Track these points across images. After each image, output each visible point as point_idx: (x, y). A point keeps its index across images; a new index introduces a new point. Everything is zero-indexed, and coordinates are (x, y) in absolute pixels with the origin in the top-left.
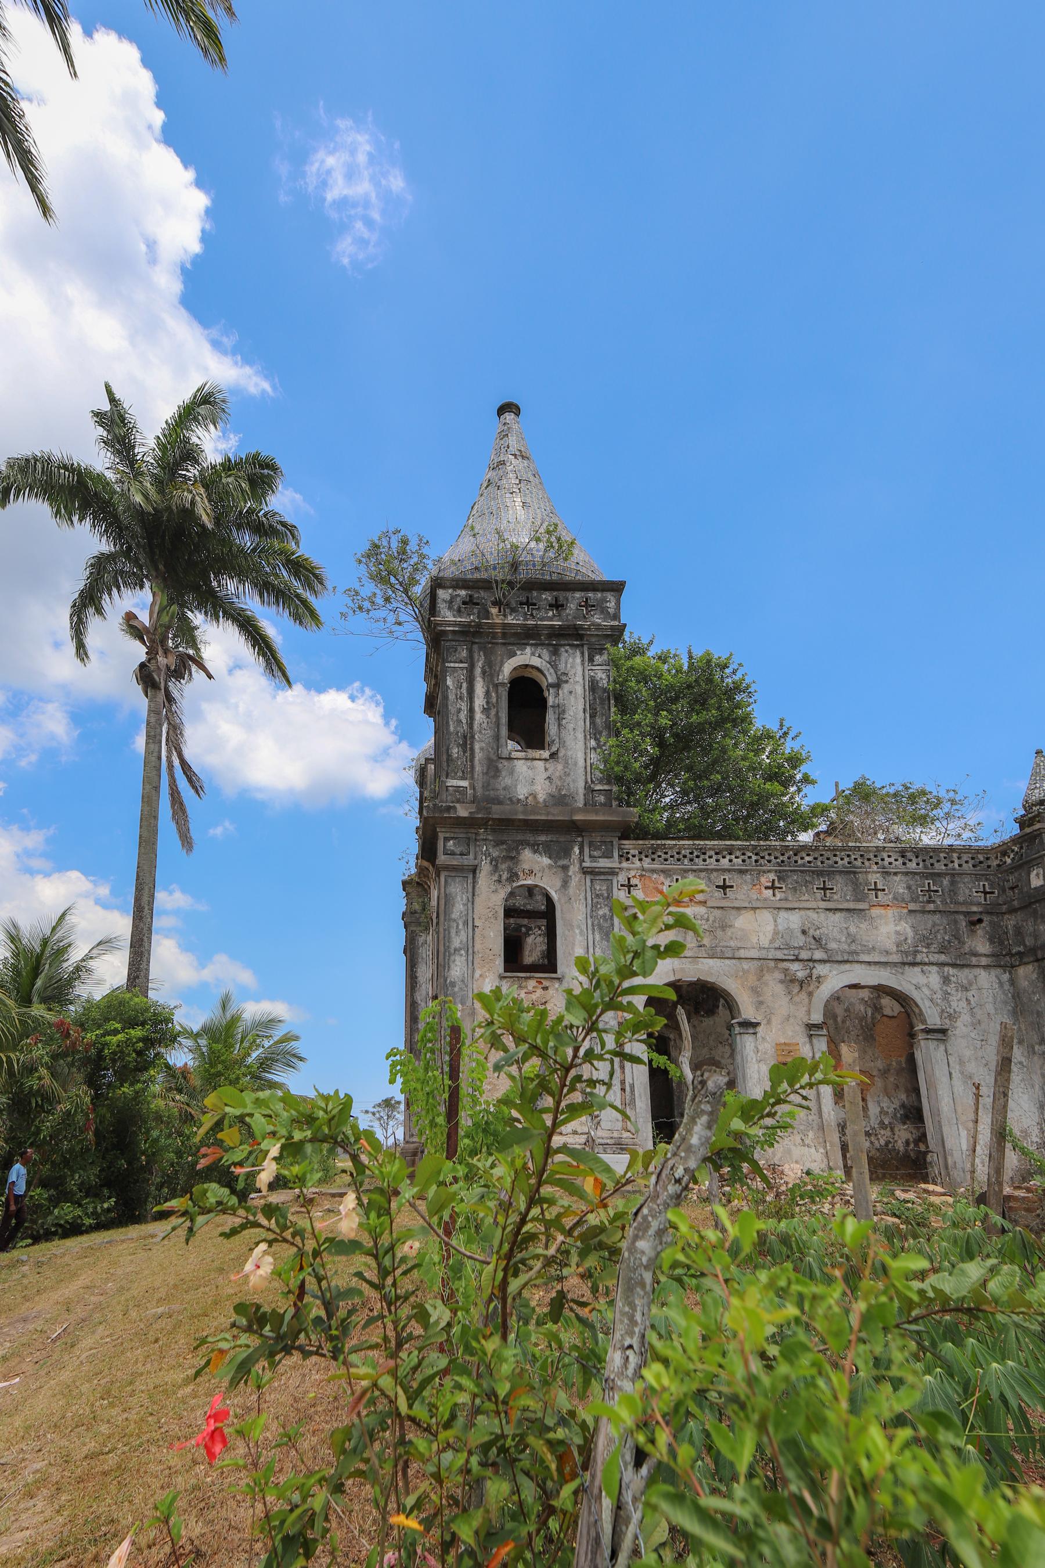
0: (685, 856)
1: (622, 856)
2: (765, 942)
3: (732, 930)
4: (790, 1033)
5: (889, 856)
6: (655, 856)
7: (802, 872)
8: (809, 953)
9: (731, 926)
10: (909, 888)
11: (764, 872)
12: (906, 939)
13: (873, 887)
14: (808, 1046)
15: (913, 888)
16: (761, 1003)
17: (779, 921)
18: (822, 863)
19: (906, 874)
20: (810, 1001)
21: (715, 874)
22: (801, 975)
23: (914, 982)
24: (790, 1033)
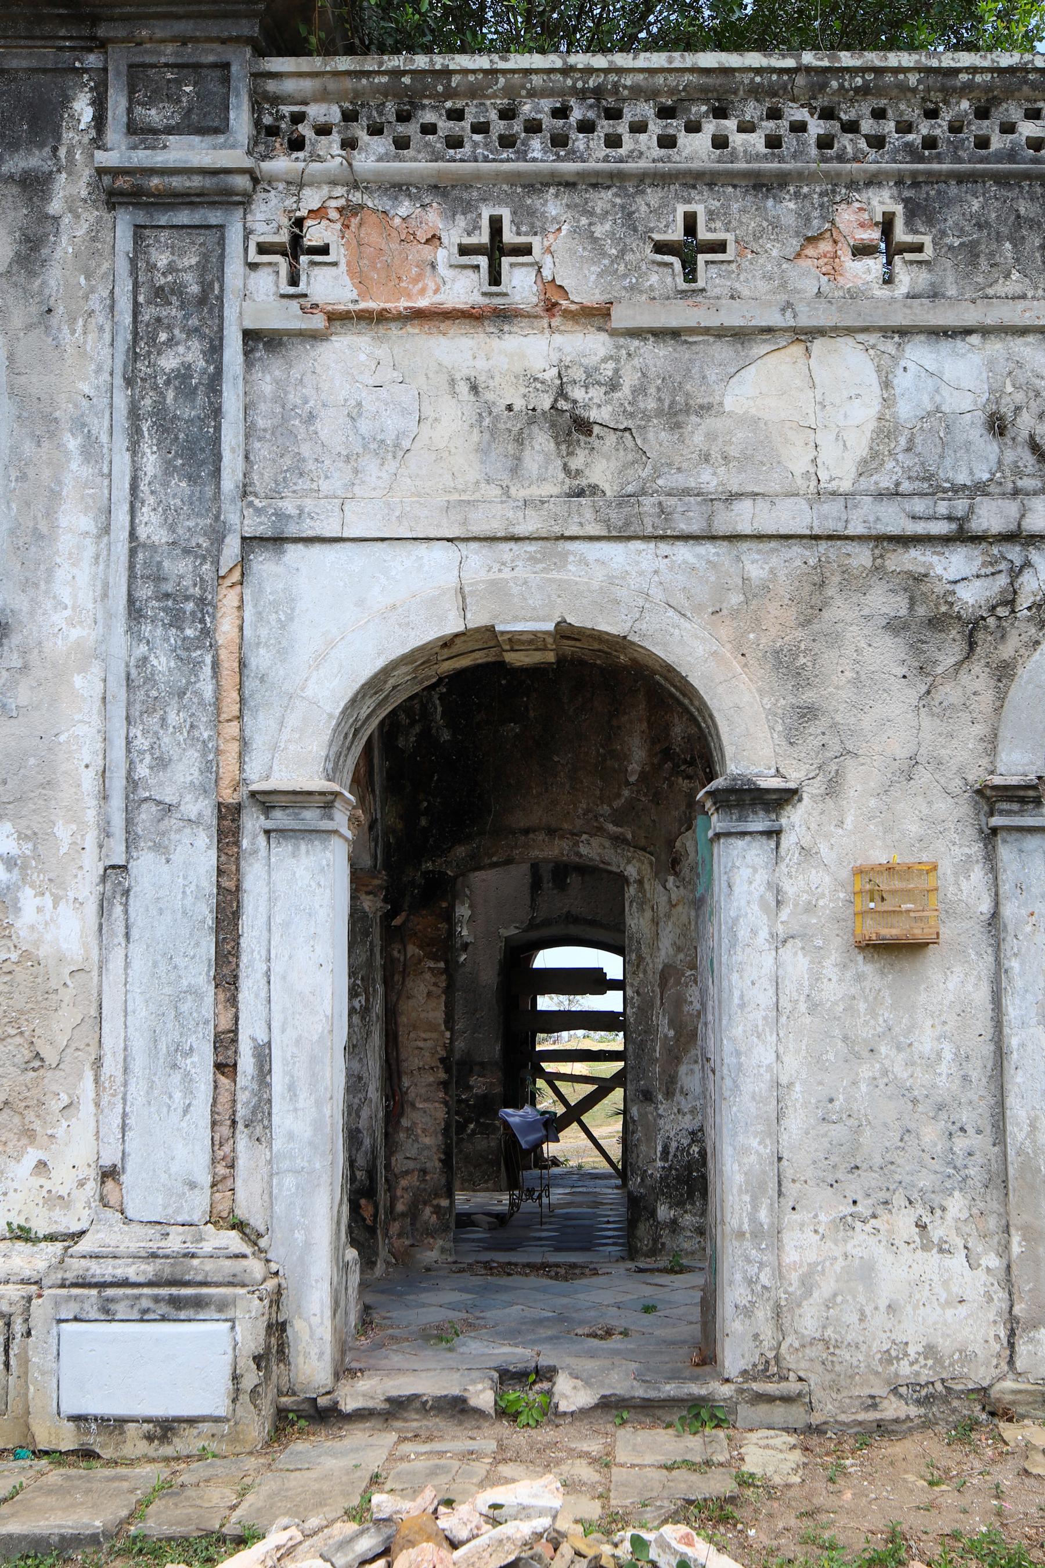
0: (533, 127)
1: (273, 131)
3: (711, 423)
4: (914, 828)
6: (411, 129)
7: (1002, 180)
8: (1012, 508)
9: (707, 408)
11: (853, 185)
14: (978, 874)
16: (807, 713)
17: (902, 382)
20: (1001, 697)
21: (653, 196)
24: (914, 828)
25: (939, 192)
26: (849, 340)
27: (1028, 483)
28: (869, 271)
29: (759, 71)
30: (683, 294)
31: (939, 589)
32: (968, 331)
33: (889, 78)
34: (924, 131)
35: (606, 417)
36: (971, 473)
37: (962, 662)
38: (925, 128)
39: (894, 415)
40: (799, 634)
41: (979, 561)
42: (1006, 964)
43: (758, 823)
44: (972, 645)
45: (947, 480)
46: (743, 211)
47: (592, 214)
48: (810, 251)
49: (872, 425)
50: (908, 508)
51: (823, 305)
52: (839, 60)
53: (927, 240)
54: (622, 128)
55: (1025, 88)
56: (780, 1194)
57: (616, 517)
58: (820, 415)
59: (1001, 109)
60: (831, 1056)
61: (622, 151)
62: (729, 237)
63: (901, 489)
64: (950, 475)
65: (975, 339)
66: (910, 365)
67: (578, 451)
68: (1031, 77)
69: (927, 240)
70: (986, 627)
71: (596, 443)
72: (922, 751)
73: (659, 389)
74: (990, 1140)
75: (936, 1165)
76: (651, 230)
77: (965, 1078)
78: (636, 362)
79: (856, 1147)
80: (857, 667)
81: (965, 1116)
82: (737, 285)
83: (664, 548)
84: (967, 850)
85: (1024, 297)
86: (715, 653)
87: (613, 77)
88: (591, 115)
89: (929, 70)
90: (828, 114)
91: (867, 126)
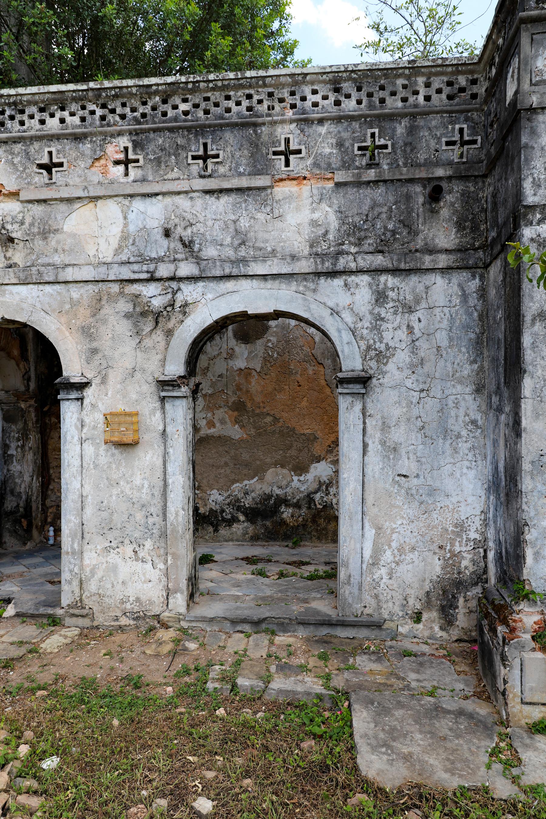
2: (107, 254)
3: (59, 236)
4: (134, 396)
5: (315, 92)
7: (171, 130)
8: (172, 267)
9: (57, 230)
10: (340, 144)
11: (112, 136)
12: (327, 232)
13: (282, 148)
14: (158, 414)
15: (347, 144)
16: (94, 351)
17: (131, 216)
18: (207, 112)
19: (338, 119)
20: (168, 344)
22: (157, 303)
23: (331, 304)
25: (146, 137)
26: (111, 200)
27: (179, 256)
28: (119, 171)
29: (74, 91)
30: (48, 185)
31: (145, 300)
32: (157, 194)
33: (125, 90)
34: (141, 111)
35: (19, 236)
36: (157, 253)
37: (153, 330)
38: (141, 110)
39: (128, 230)
40: (91, 320)
41: (160, 289)
42: (168, 450)
43: (74, 395)
44: (157, 323)
45: (148, 256)
46: (70, 149)
47: (14, 154)
48: (97, 164)
49: (119, 235)
50: (131, 268)
51: (99, 187)
52: (103, 84)
53: (141, 157)
54: (25, 117)
55: (180, 90)
56: (83, 538)
57: (22, 275)
58: (100, 231)
59: (172, 99)
60: (102, 486)
61: (25, 127)
62: (64, 161)
63: (130, 260)
64: (149, 254)
65: (160, 197)
66: (135, 210)
67: (10, 250)
68: (181, 85)
69: (141, 157)
70: (163, 315)
71: (16, 246)
72: (138, 366)
73: (39, 224)
74: (162, 519)
75: (141, 528)
76: (36, 159)
77: (153, 494)
78: (31, 213)
79: (111, 521)
80: (113, 333)
81: (152, 510)
82: (68, 180)
83: (41, 287)
84: (154, 405)
85: (179, 179)
86: (58, 329)
87: (19, 97)
88: (13, 113)
89: (140, 86)
90: (104, 106)
91: (119, 110)
